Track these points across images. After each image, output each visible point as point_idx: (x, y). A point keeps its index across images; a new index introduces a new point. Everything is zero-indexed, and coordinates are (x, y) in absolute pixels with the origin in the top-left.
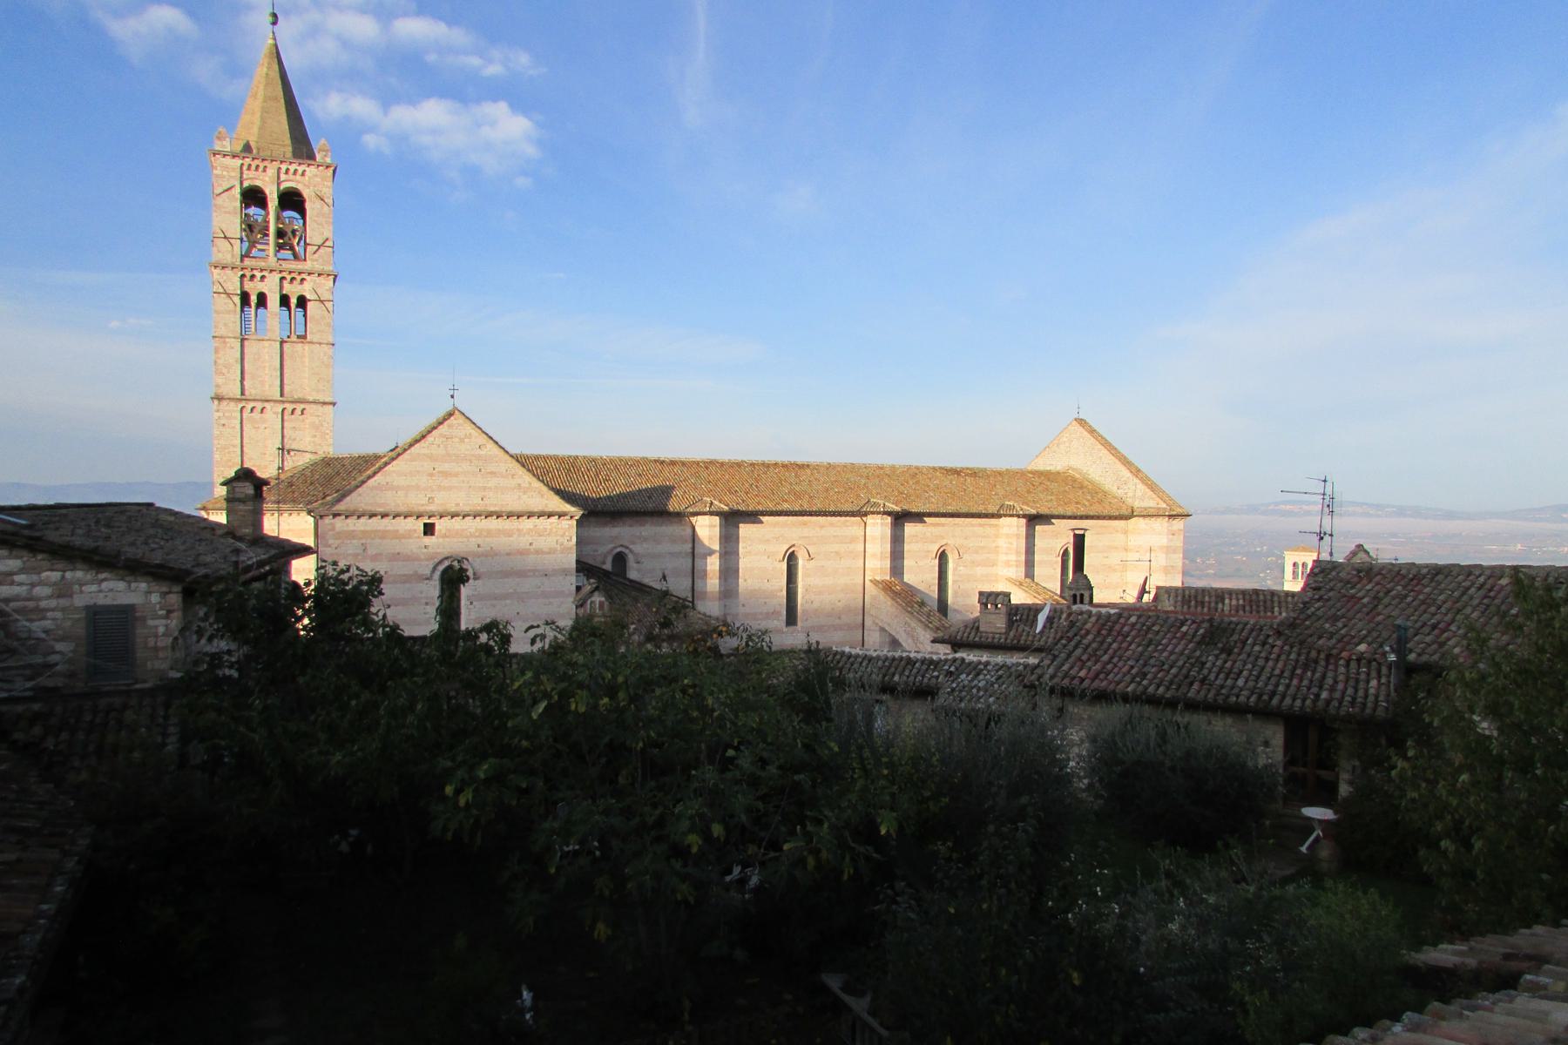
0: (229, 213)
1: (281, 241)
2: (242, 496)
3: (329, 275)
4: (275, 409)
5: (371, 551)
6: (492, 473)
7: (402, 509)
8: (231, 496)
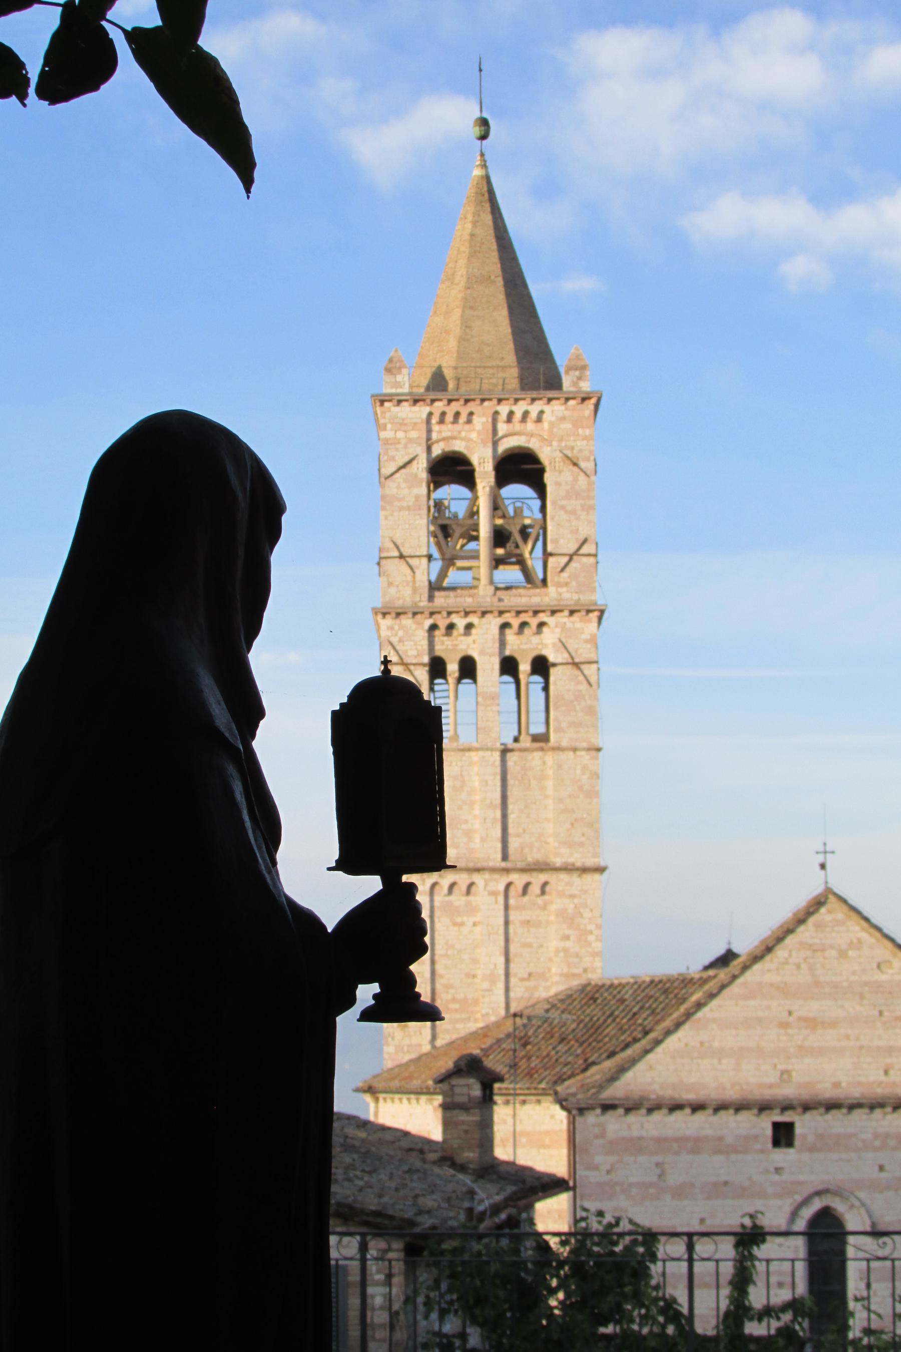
0: (409, 508)
1: (500, 551)
2: (464, 1099)
3: (589, 611)
4: (492, 886)
5: (674, 1178)
7: (732, 1094)
8: (449, 1100)
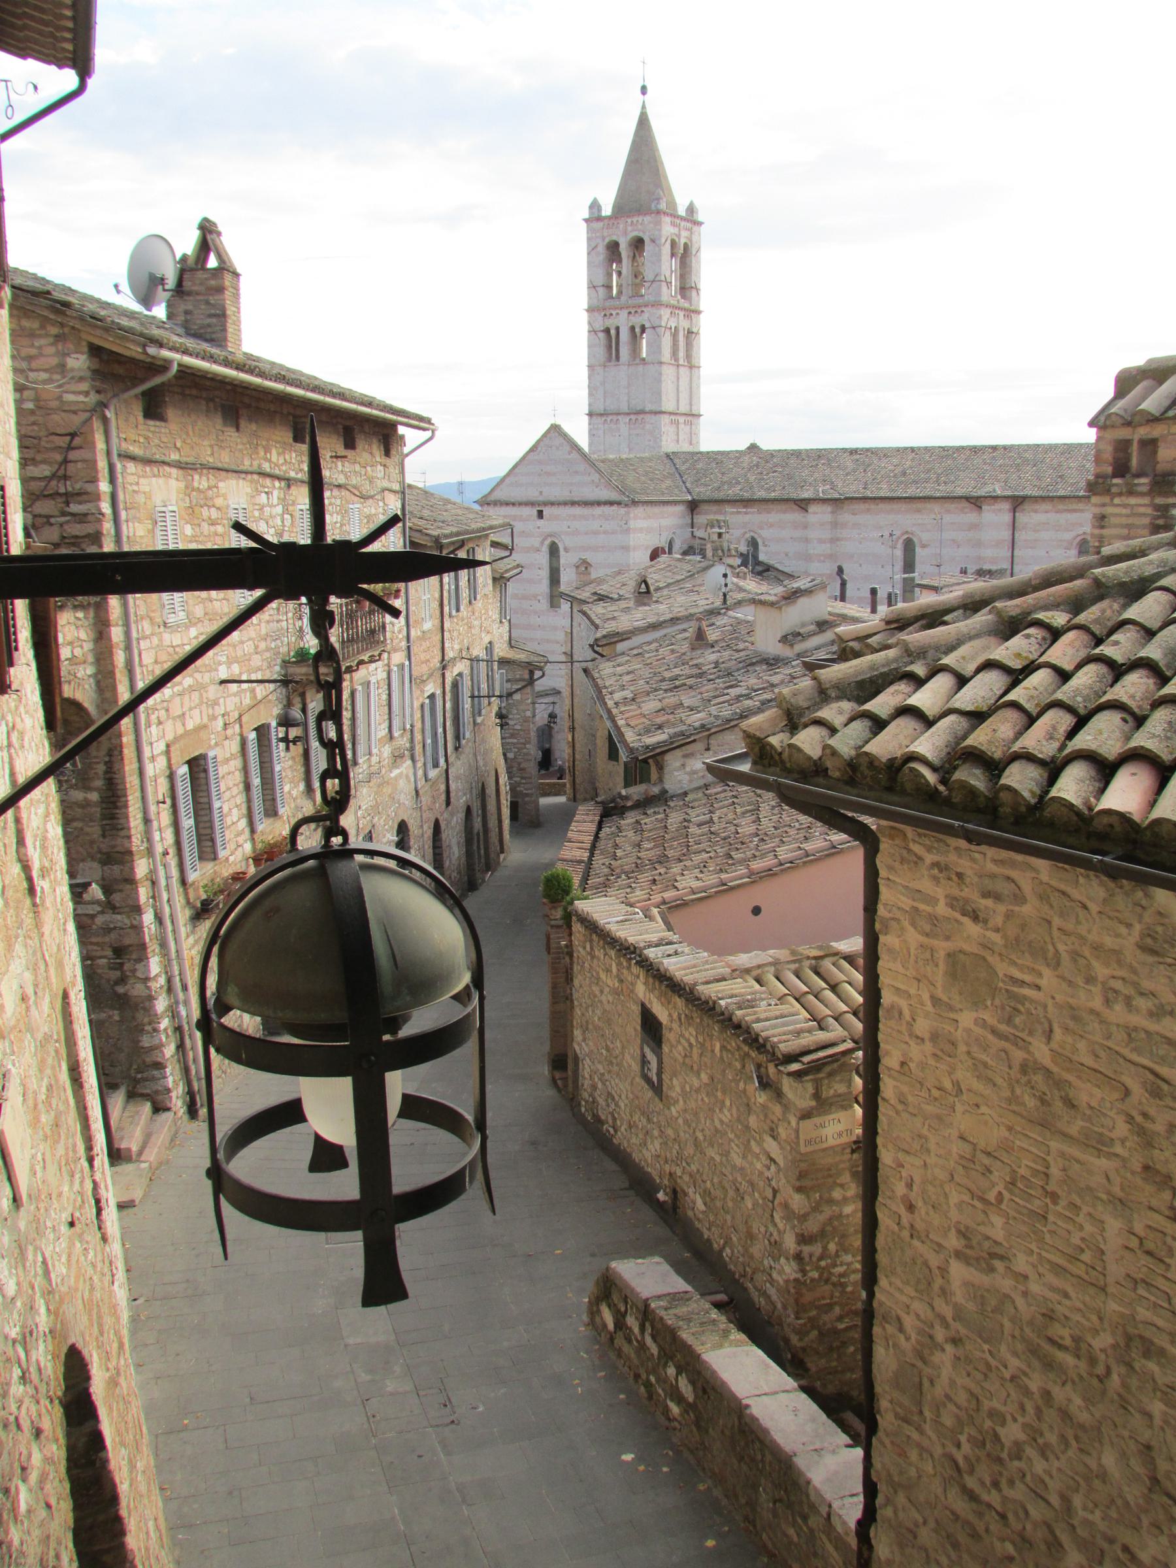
6: (576, 472)
